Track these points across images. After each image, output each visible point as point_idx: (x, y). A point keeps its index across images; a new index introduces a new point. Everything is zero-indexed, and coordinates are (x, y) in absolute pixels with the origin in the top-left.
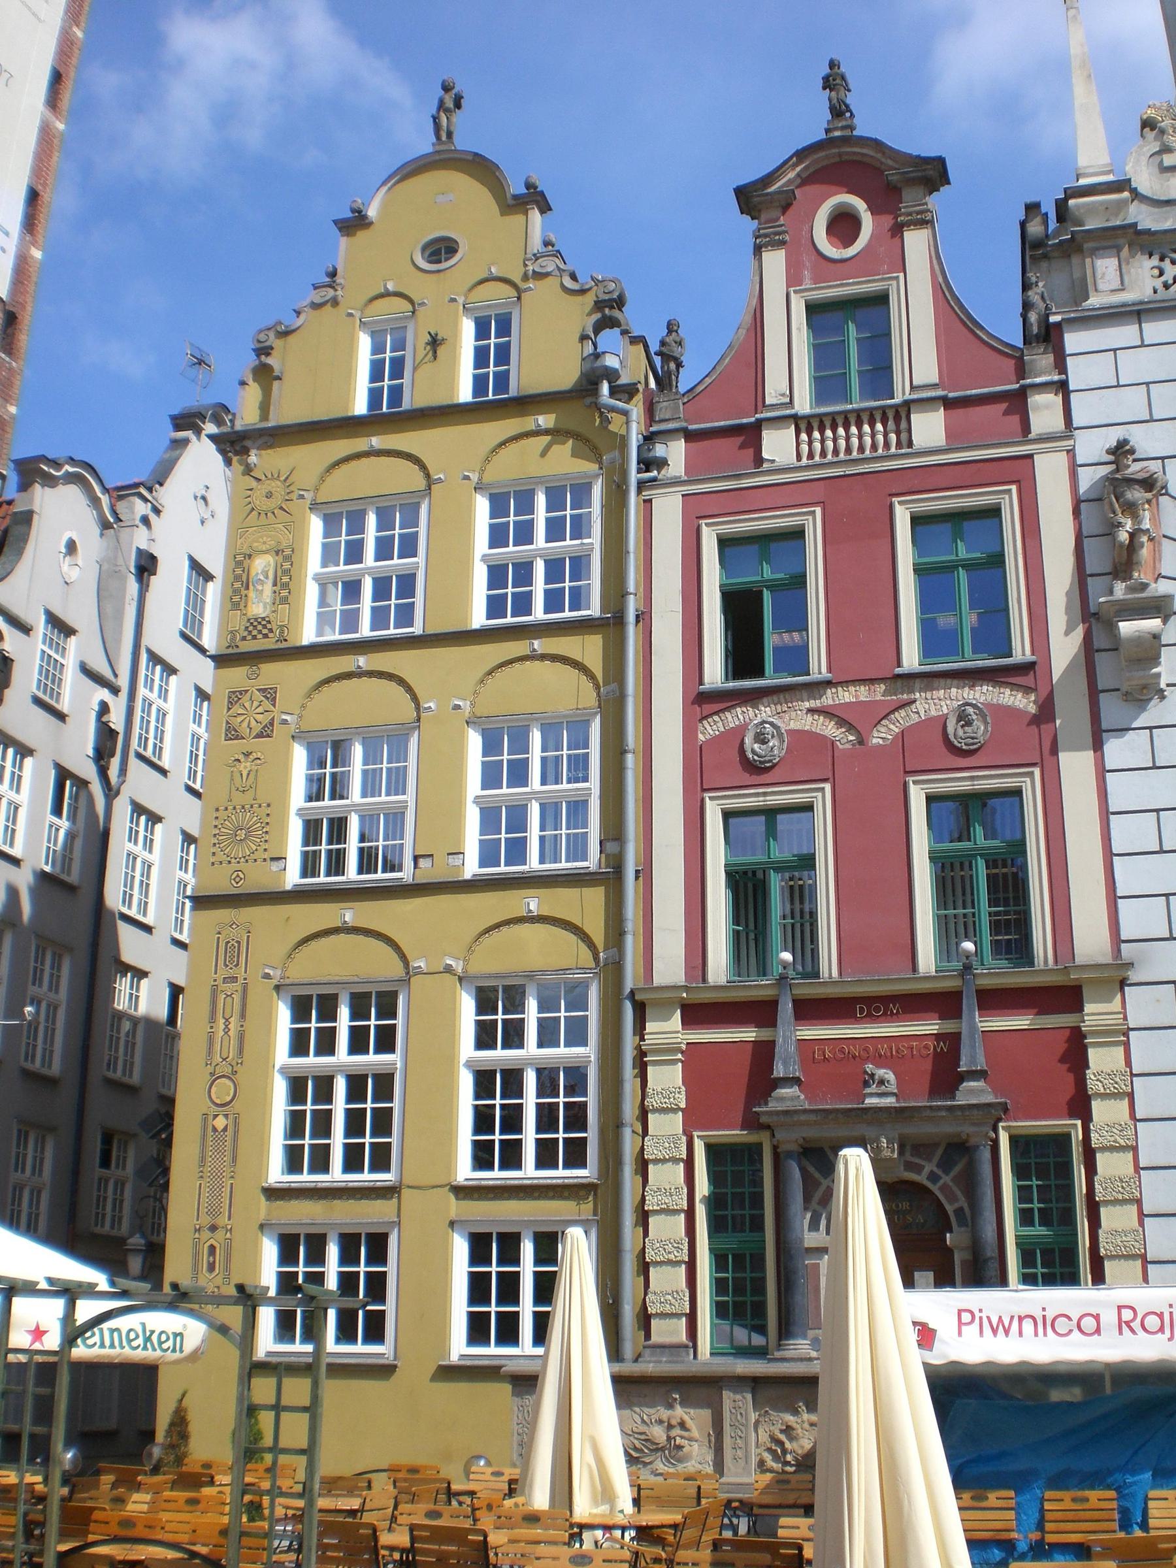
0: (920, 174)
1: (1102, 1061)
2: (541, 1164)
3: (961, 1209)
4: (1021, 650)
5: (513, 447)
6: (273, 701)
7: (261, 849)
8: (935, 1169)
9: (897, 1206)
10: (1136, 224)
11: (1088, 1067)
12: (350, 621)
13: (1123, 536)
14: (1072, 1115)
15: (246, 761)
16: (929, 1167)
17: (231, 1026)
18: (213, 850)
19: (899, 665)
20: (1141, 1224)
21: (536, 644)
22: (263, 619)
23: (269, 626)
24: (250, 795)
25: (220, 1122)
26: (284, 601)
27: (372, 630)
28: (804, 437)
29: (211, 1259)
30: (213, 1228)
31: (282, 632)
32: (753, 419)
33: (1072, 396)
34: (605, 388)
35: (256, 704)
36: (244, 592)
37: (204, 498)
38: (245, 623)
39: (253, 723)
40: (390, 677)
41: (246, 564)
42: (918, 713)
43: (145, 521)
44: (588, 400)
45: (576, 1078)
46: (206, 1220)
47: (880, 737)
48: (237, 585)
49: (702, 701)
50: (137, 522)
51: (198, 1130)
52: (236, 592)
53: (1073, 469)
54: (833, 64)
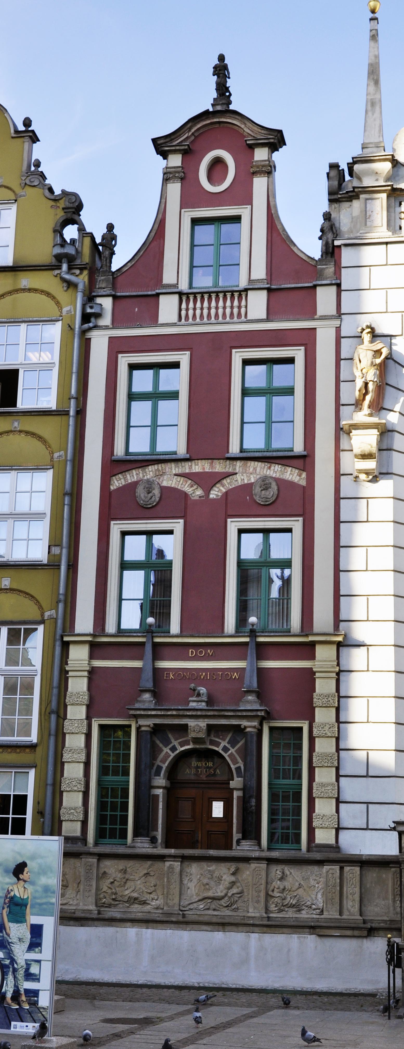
1: (324, 686)
4: (299, 448)
9: (206, 764)
11: (315, 691)
16: (223, 744)
19: (228, 452)
20: (337, 780)
32: (154, 293)
33: (343, 293)
42: (237, 481)
44: (57, 272)
47: (213, 494)
49: (113, 465)
53: (339, 338)
54: (221, 58)
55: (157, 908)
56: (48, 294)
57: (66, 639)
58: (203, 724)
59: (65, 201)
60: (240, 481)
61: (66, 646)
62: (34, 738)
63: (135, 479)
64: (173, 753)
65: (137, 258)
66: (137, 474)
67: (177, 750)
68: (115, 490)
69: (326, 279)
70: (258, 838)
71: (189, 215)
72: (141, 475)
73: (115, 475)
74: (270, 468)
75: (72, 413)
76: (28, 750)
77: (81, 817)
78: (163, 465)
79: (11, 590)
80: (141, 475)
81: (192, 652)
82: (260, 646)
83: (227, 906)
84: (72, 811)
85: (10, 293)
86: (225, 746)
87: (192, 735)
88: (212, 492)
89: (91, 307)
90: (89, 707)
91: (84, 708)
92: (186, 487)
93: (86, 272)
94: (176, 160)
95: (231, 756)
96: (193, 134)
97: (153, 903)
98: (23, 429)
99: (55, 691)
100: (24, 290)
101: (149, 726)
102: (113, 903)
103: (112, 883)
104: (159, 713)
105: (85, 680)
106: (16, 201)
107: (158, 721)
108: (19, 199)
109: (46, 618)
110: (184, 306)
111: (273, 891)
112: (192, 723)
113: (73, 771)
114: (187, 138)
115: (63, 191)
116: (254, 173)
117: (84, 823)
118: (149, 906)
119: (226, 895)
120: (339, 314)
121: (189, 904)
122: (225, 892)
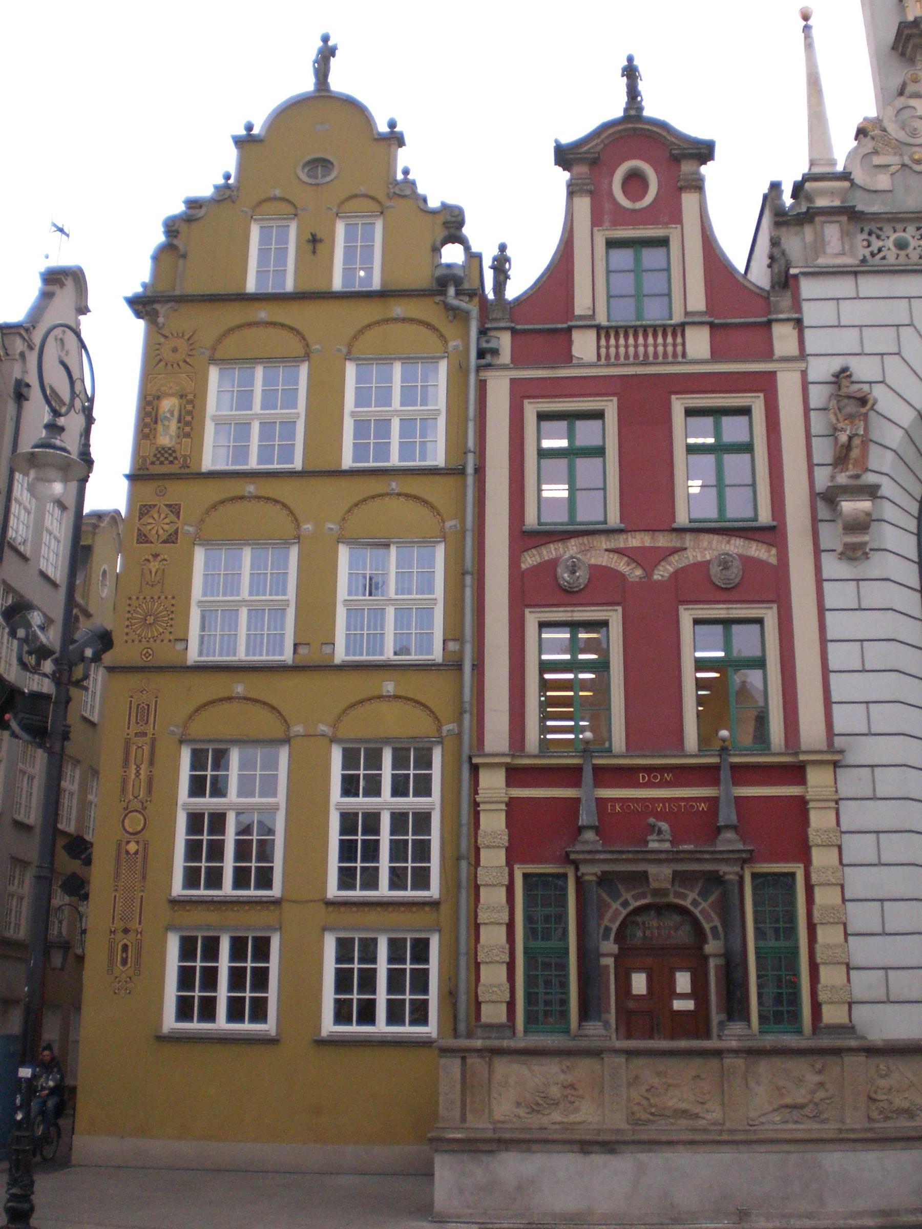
0: (695, 151)
1: (819, 820)
2: (393, 886)
3: (716, 927)
4: (765, 517)
8: (697, 897)
10: (855, 206)
12: (241, 452)
13: (843, 438)
14: (794, 860)
15: (154, 560)
16: (692, 896)
17: (142, 772)
18: (127, 630)
21: (394, 485)
22: (170, 449)
25: (132, 847)
26: (188, 435)
27: (259, 463)
28: (603, 342)
29: (124, 955)
30: (126, 931)
31: (185, 460)
32: (565, 326)
34: (452, 291)
35: (163, 516)
36: (153, 426)
37: (61, 340)
38: (153, 451)
39: (161, 532)
43: (22, 355)
44: (438, 299)
45: (423, 820)
46: (119, 925)
48: (148, 420)
49: (524, 538)
50: (17, 357)
52: (146, 425)
53: (805, 385)
54: (630, 59)
55: (714, 1124)
56: (428, 325)
57: (476, 760)
58: (666, 871)
60: (691, 559)
61: (475, 769)
62: (434, 891)
63: (554, 555)
66: (556, 549)
68: (528, 569)
69: (781, 312)
70: (747, 1018)
72: (561, 551)
73: (527, 550)
74: (728, 542)
75: (470, 470)
76: (427, 909)
77: (507, 997)
78: (589, 537)
79: (396, 697)
80: (561, 551)
81: (644, 778)
82: (734, 767)
83: (815, 1117)
84: (495, 989)
85: (378, 323)
86: (694, 899)
87: (654, 885)
88: (656, 572)
89: (488, 342)
91: (502, 853)
92: (622, 565)
93: (476, 300)
95: (703, 912)
96: (602, 141)
97: (709, 1116)
98: (404, 491)
99: (464, 830)
101: (595, 874)
102: (652, 1118)
103: (647, 1090)
105: (503, 816)
106: (382, 213)
107: (607, 867)
109: (444, 734)
110: (603, 342)
111: (876, 1092)
112: (652, 870)
113: (493, 937)
114: (597, 145)
116: (681, 189)
117: (511, 1006)
118: (704, 1122)
119: (811, 1101)
120: (803, 355)
121: (760, 1116)
122: (809, 1097)
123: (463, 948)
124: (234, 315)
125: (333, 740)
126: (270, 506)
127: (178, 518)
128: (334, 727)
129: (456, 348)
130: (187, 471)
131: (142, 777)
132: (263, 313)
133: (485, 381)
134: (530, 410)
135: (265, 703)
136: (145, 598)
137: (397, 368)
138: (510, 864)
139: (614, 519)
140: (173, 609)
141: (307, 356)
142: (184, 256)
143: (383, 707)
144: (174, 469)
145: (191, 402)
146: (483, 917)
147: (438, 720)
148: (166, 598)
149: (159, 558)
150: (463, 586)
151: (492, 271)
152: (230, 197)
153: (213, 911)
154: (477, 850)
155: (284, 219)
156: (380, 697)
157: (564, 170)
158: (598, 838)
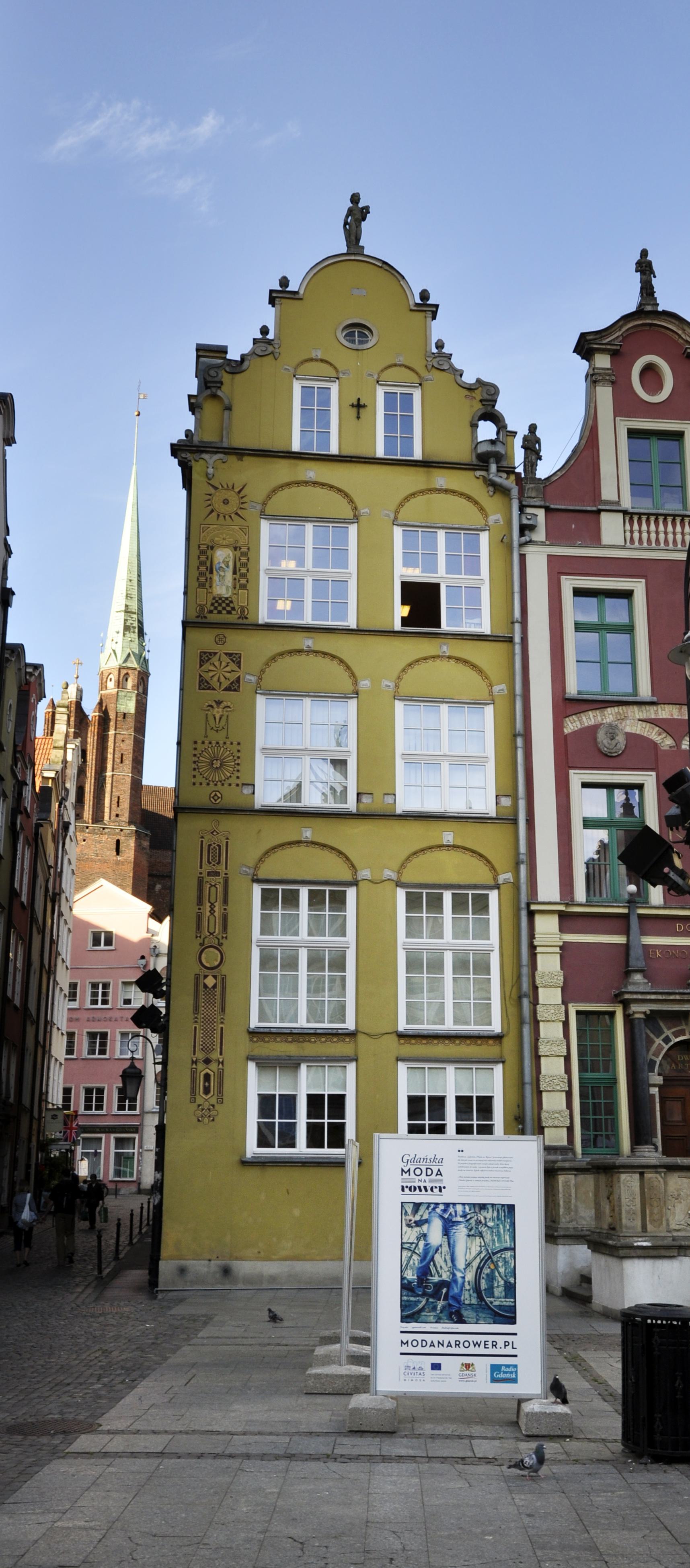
5: (420, 499)
6: (239, 664)
7: (234, 777)
15: (218, 707)
17: (216, 909)
21: (445, 648)
22: (227, 599)
23: (232, 605)
24: (224, 732)
26: (243, 587)
30: (207, 1061)
32: (594, 509)
34: (493, 467)
40: (333, 657)
41: (209, 552)
44: (478, 473)
46: (200, 1055)
48: (203, 569)
49: (566, 705)
51: (191, 988)
52: (201, 574)
56: (469, 498)
59: (482, 391)
61: (531, 914)
62: (496, 1027)
64: (667, 1044)
65: (567, 467)
67: (671, 1041)
71: (625, 424)
72: (599, 718)
75: (517, 639)
76: (491, 1042)
77: (568, 1124)
78: (624, 707)
79: (455, 847)
84: (557, 1115)
85: (422, 492)
90: (564, 989)
92: (653, 734)
93: (513, 477)
94: (603, 361)
100: (439, 490)
101: (645, 1013)
104: (660, 997)
108: (424, 383)
113: (553, 1067)
115: (479, 381)
117: (570, 1129)
123: (527, 1078)
124: (283, 471)
125: (399, 884)
126: (328, 660)
127: (239, 667)
128: (398, 872)
129: (497, 521)
130: (245, 621)
131: (216, 914)
132: (312, 471)
133: (524, 555)
134: (568, 584)
135: (332, 848)
136: (210, 743)
137: (441, 535)
138: (565, 1002)
139: (645, 690)
140: (239, 754)
141: (356, 518)
142: (229, 408)
143: (442, 855)
144: (233, 618)
145: (244, 554)
146: (543, 1049)
147: (495, 870)
148: (232, 743)
149: (222, 705)
150: (516, 748)
151: (523, 450)
152: (272, 353)
153: (291, 1042)
154: (535, 988)
155: (327, 381)
156: (441, 846)
157: (582, 358)
158: (646, 981)
